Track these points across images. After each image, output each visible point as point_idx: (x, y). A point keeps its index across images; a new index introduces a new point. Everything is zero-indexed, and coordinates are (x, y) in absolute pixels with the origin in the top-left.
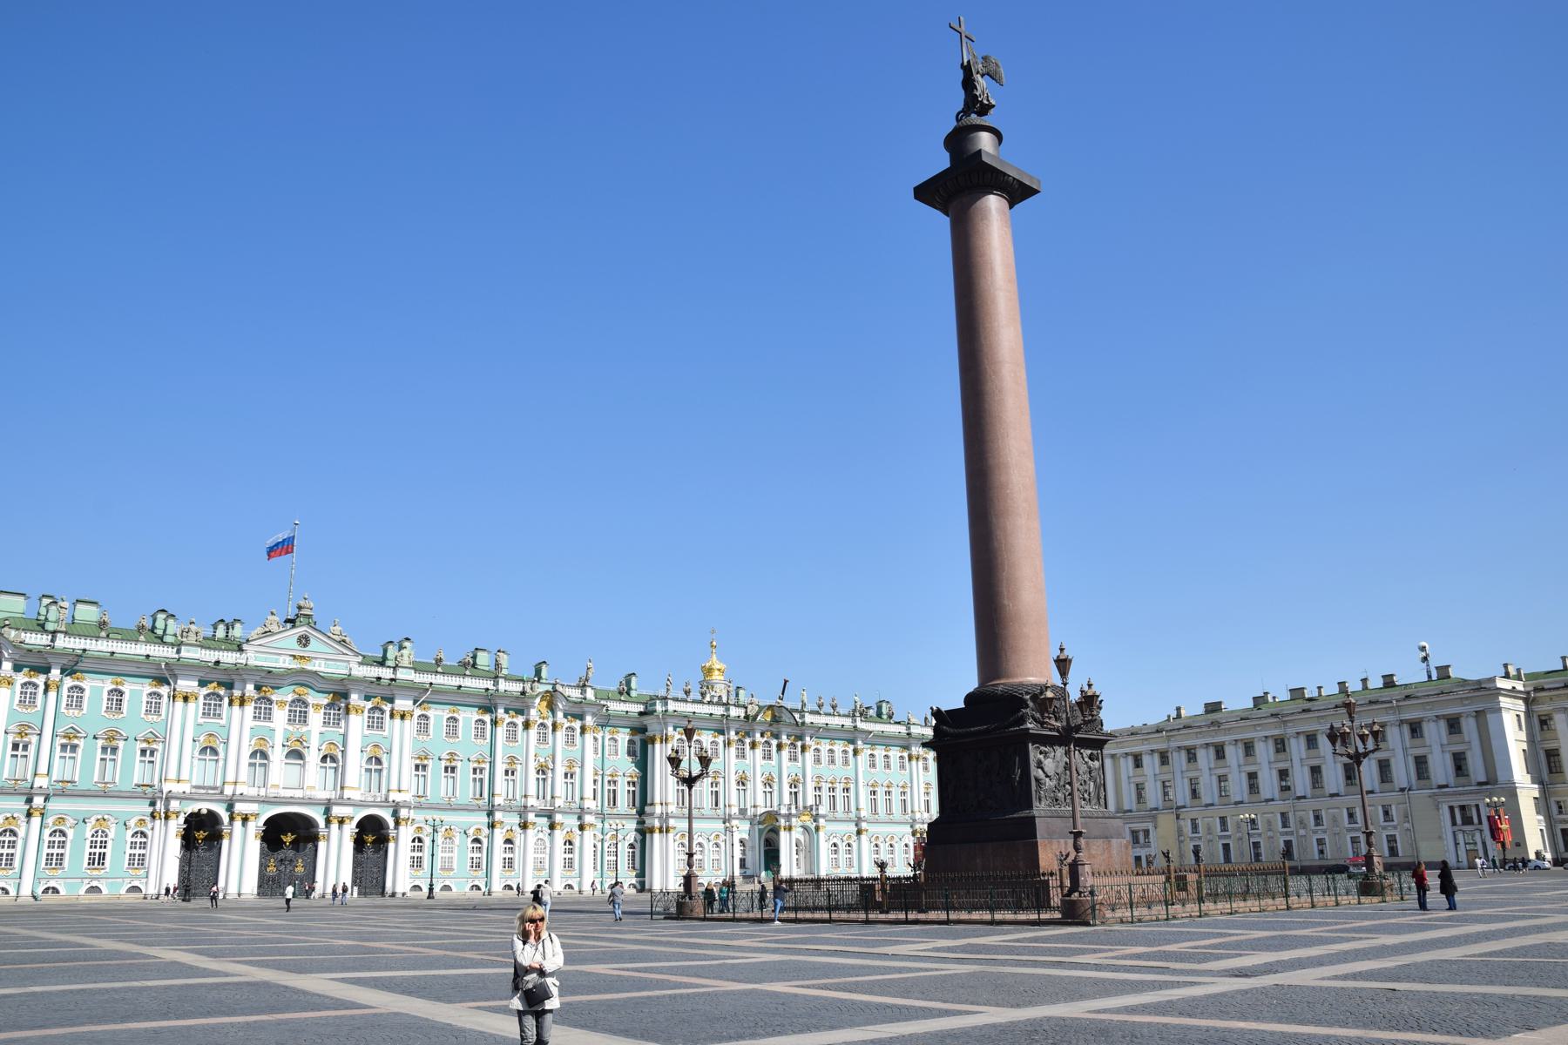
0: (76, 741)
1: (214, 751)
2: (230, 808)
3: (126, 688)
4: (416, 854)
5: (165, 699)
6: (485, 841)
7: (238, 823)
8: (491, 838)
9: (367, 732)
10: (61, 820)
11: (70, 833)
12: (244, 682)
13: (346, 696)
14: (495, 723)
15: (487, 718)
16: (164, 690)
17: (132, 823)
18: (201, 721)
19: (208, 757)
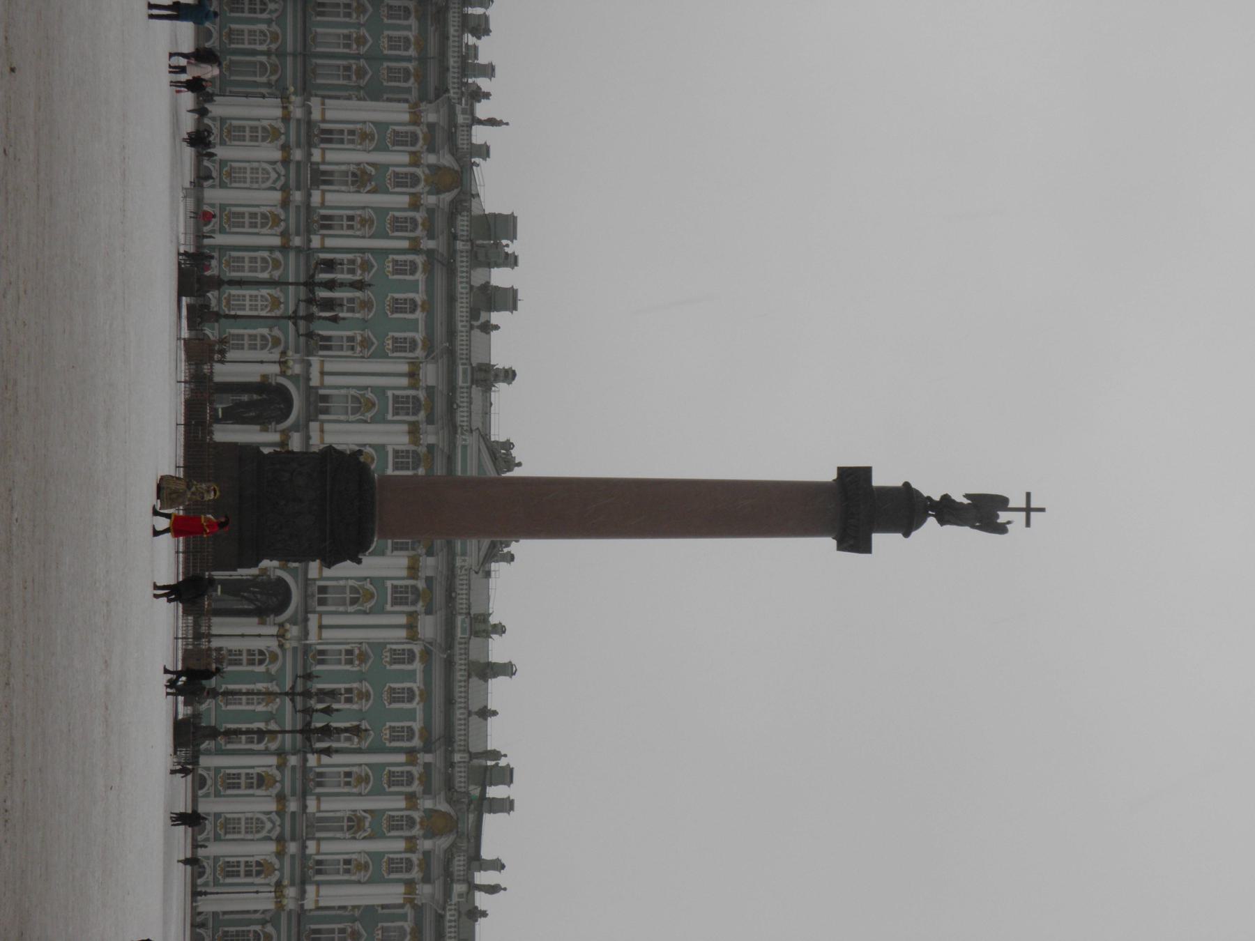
0: (359, 272)
1: (355, 411)
2: (295, 427)
3: (419, 315)
4: (244, 657)
5: (411, 355)
6: (261, 747)
7: (275, 437)
8: (266, 752)
12: (437, 433)
14: (411, 752)
15: (416, 742)
16: (419, 353)
17: (276, 332)
18: (390, 393)
19: (350, 405)
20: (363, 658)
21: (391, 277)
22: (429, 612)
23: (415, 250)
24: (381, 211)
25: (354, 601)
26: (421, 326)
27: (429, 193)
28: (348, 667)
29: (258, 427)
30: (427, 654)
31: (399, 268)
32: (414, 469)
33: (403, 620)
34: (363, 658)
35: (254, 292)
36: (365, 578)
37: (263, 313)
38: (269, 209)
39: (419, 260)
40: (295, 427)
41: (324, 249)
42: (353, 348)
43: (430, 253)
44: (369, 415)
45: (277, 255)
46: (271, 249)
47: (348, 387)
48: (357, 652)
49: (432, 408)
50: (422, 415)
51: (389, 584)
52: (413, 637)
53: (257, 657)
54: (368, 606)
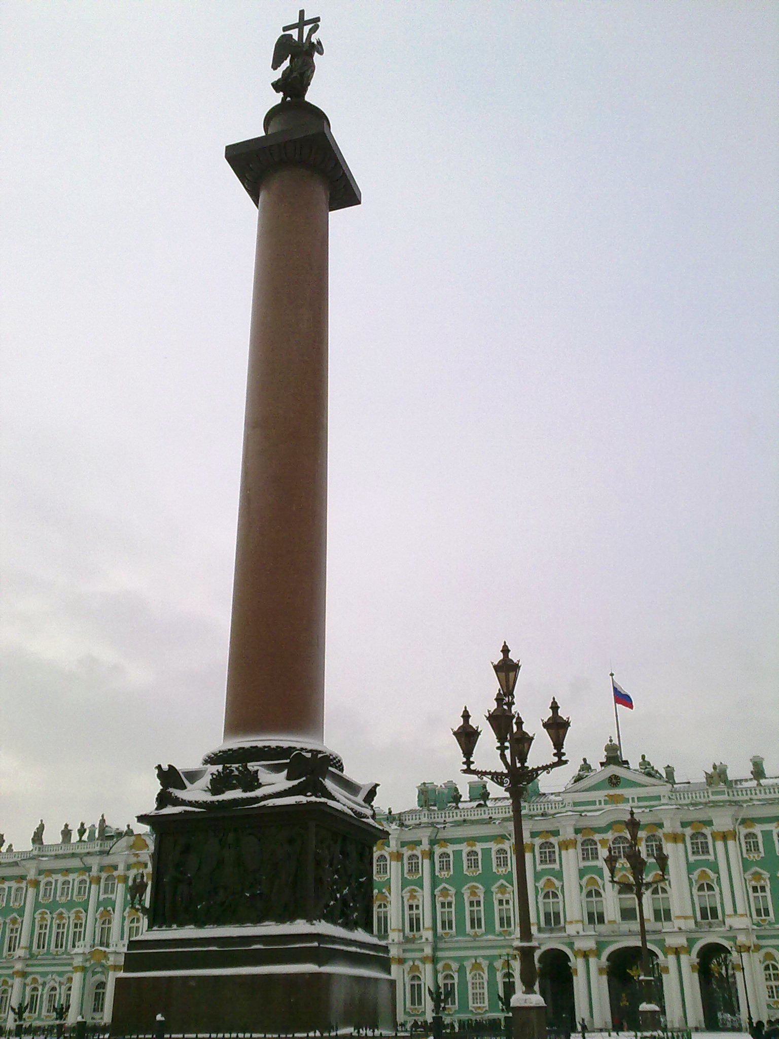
0: (449, 899)
1: (555, 895)
9: (692, 858)
10: (447, 967)
11: (456, 976)
13: (660, 825)
18: (539, 868)
20: (757, 876)
21: (452, 873)
22: (709, 823)
23: (431, 855)
24: (405, 883)
25: (710, 888)
26: (486, 845)
27: (389, 846)
28: (768, 889)
29: (574, 978)
30: (744, 822)
31: (445, 866)
32: (596, 844)
33: (720, 844)
34: (757, 876)
35: (470, 985)
36: (690, 879)
37: (486, 976)
38: (406, 975)
39: (438, 850)
40: (571, 945)
41: (434, 928)
42: (507, 902)
43: (433, 842)
44: (557, 883)
45: (440, 966)
46: (436, 972)
47: (537, 903)
48: (754, 883)
49: (547, 832)
50: (553, 840)
51: (692, 858)
52: (734, 835)
53: (772, 972)
54: (712, 875)
